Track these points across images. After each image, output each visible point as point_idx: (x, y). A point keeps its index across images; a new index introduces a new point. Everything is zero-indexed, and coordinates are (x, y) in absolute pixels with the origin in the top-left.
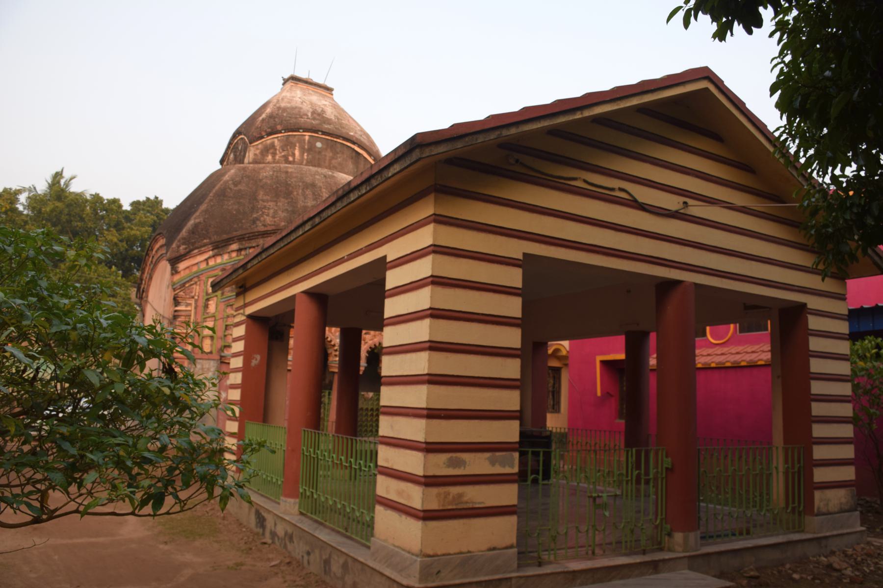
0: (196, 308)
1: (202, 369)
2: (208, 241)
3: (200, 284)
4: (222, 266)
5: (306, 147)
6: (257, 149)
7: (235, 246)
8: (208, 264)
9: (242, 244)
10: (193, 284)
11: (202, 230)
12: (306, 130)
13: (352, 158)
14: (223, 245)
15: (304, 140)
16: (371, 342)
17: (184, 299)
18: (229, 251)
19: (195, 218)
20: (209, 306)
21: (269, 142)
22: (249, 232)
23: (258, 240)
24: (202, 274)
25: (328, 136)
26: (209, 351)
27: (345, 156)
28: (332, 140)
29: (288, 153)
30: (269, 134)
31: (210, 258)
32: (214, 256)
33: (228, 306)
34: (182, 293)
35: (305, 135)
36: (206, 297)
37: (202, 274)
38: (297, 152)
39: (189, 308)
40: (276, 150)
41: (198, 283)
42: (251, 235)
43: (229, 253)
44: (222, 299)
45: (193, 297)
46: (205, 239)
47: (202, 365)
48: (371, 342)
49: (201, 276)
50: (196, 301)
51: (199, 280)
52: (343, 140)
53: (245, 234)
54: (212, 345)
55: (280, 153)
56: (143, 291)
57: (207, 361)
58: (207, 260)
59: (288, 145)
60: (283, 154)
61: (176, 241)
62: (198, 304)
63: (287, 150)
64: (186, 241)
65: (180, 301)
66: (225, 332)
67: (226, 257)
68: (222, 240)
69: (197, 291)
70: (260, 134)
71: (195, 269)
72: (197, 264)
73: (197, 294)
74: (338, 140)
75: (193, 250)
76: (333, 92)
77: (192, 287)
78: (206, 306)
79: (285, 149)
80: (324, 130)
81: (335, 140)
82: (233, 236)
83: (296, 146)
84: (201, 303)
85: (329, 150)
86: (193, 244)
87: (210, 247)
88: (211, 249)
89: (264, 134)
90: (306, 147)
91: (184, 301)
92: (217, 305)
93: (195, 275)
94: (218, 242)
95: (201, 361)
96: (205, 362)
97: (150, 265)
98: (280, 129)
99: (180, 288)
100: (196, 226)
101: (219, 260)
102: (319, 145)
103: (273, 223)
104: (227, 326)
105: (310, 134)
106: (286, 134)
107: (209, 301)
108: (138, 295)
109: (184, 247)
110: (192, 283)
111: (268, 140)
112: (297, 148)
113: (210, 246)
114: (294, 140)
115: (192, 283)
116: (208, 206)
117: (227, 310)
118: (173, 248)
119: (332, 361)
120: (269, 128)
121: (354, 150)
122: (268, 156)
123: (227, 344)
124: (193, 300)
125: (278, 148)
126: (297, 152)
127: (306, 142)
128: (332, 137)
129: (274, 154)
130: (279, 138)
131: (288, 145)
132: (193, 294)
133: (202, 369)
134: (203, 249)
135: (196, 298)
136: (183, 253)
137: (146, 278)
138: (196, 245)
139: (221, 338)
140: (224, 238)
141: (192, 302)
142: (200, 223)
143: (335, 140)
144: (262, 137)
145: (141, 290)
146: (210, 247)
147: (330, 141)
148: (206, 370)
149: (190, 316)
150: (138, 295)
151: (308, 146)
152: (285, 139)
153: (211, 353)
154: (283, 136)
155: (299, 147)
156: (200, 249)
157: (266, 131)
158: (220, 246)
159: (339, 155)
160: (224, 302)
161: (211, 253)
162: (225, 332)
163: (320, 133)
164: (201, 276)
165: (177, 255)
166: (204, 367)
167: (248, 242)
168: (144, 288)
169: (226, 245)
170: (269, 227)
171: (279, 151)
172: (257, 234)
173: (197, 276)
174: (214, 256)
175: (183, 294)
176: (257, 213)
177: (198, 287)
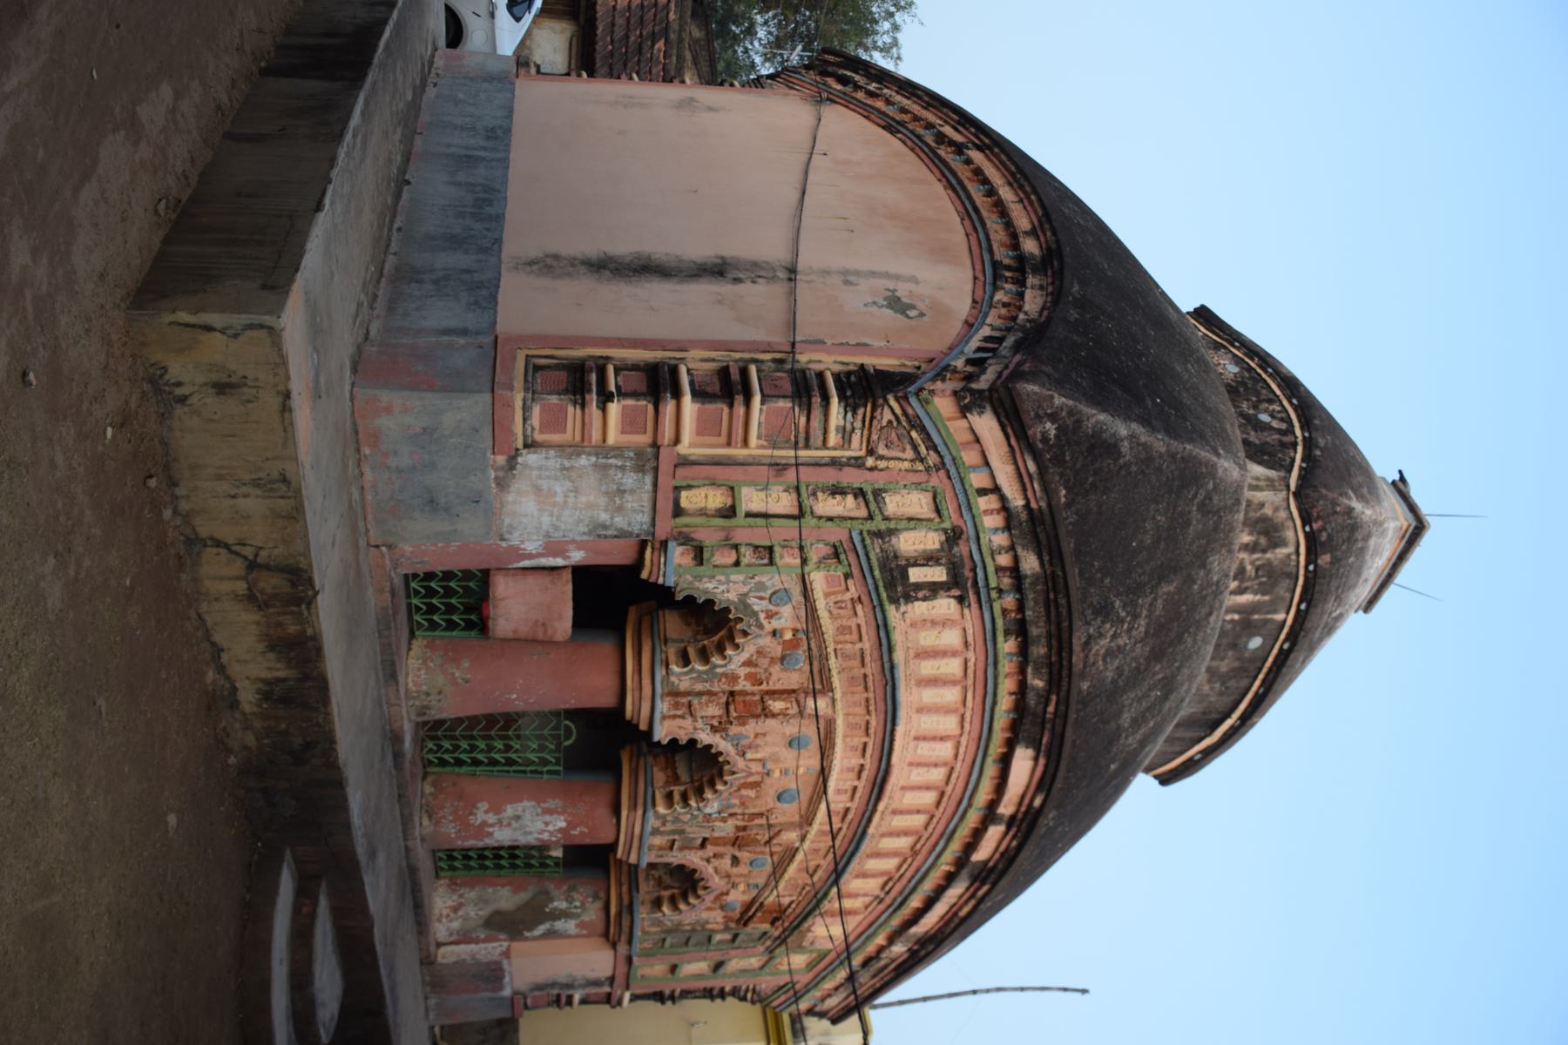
0: (834, 463)
1: (621, 492)
2: (1063, 500)
3: (917, 471)
4: (971, 532)
5: (1256, 617)
6: (1276, 509)
7: (1030, 563)
8: (982, 492)
11: (1096, 473)
12: (1301, 618)
13: (1204, 713)
14: (1042, 537)
15: (1275, 611)
16: (710, 870)
17: (868, 424)
18: (1019, 550)
19: (1132, 436)
20: (838, 497)
21: (1290, 534)
22: (1075, 606)
23: (1042, 624)
24: (949, 478)
26: (684, 503)
27: (1213, 699)
28: (1260, 669)
29: (1250, 579)
30: (1311, 538)
31: (1003, 498)
32: (1005, 508)
33: (834, 546)
34: (888, 415)
35: (1288, 612)
36: (868, 489)
37: (949, 478)
39: (833, 438)
40: (1264, 551)
41: (920, 467)
42: (1064, 611)
43: (1012, 548)
44: (861, 533)
45: (871, 452)
47: (632, 491)
48: (710, 870)
49: (942, 473)
50: (857, 463)
51: (928, 469)
52: (1257, 693)
53: (1068, 596)
54: (703, 512)
55: (1252, 563)
56: (844, 81)
57: (647, 504)
58: (996, 489)
59: (1270, 577)
60: (1249, 567)
61: (1071, 403)
62: (846, 469)
63: (1257, 577)
64: (1071, 430)
65: (861, 411)
66: (747, 545)
67: (1001, 539)
68: (1057, 537)
69: (892, 464)
70: (1319, 517)
71: (970, 457)
72: (987, 464)
73: (882, 464)
74: (1257, 683)
75: (1037, 458)
76: (1361, 612)
77: (908, 447)
78: (837, 491)
79: (1260, 573)
80: (1292, 656)
81: (1261, 676)
82: (1068, 568)
84: (852, 477)
85: (1236, 664)
86: (1058, 460)
88: (1034, 505)
89: (1315, 526)
90: (1256, 617)
91: (858, 424)
92: (844, 518)
93: (948, 460)
94: (1055, 528)
95: (649, 487)
96: (646, 498)
97: (930, 126)
98: (1320, 561)
99: (905, 413)
101: (992, 521)
102: (1256, 643)
103: (1091, 660)
104: (770, 549)
105: (1289, 622)
106: (1302, 572)
107: (856, 497)
108: (831, 58)
109: (1053, 432)
110: (923, 449)
111: (1295, 535)
112: (1258, 597)
113: (1043, 504)
114: (1282, 590)
115: (923, 449)
116: (1161, 455)
117: (821, 546)
118: (1052, 397)
119: (650, 782)
120: (1329, 535)
121: (1227, 715)
122: (1251, 534)
123: (706, 555)
124: (863, 453)
125: (1269, 555)
127: (1269, 616)
128: (1270, 669)
129: (1251, 548)
130: (1294, 557)
131: (1269, 577)
132: (882, 450)
133: (621, 492)
134: (1036, 486)
135: (870, 462)
136: (1030, 433)
137: (888, 102)
138: (1054, 472)
140: (1064, 544)
141: (856, 449)
142: (1119, 455)
143: (1261, 676)
144: (1306, 520)
145: (849, 74)
147: (1258, 665)
148: (618, 501)
149: (807, 446)
150: (831, 58)
153: (678, 511)
155: (1258, 602)
156: (1035, 476)
157: (1324, 529)
158: (1038, 530)
159: (1217, 685)
160: (851, 538)
161: (1017, 502)
162: (747, 545)
163: (1286, 646)
164: (942, 473)
165: (1029, 415)
166: (628, 497)
167: (1041, 599)
168: (857, 87)
170: (1082, 655)
171: (1258, 559)
172: (1065, 624)
173: (943, 464)
174: (1005, 508)
175: (884, 423)
176: (1124, 607)
177: (906, 465)
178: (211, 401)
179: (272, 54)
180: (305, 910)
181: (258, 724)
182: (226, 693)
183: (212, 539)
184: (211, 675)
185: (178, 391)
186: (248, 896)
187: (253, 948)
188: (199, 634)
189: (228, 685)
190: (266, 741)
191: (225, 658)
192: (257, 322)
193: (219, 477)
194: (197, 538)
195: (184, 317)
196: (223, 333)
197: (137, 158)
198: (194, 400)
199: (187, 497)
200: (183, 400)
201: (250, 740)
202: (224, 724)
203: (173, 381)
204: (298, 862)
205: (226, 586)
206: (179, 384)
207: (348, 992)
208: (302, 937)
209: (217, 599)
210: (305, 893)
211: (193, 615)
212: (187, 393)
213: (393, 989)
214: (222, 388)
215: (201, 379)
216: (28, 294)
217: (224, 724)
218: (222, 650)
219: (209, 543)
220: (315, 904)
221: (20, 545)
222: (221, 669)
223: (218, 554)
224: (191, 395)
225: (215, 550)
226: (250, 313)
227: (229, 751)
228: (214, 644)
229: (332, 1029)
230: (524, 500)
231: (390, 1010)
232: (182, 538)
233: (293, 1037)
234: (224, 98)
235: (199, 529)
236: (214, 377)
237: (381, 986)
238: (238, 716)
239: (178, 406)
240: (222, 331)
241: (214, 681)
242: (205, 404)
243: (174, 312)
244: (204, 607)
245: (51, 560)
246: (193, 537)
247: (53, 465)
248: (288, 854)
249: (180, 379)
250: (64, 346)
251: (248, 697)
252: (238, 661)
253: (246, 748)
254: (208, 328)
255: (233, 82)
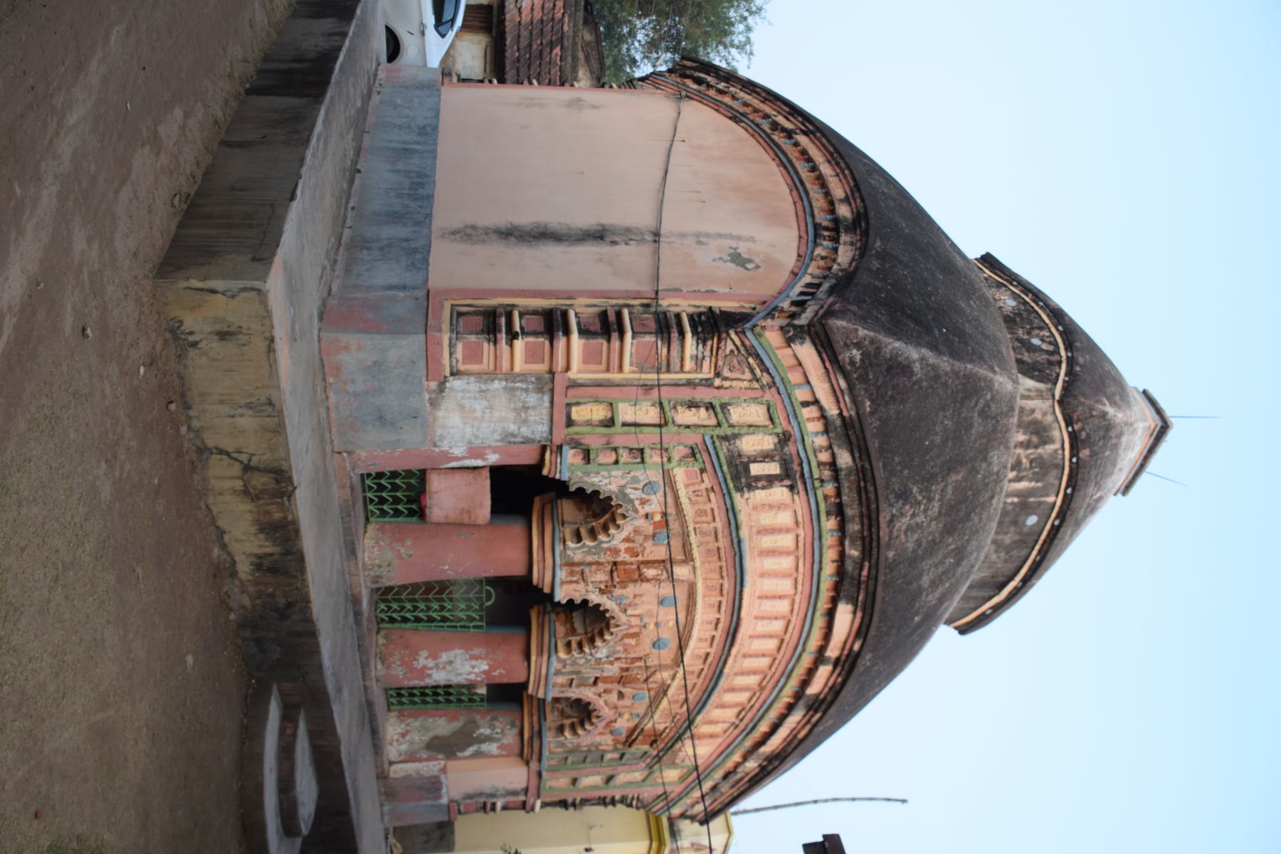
0: (689, 383)
1: (526, 408)
2: (868, 409)
4: (798, 435)
5: (1032, 500)
6: (1045, 414)
7: (844, 459)
8: (805, 404)
9: (848, 475)
10: (752, 371)
11: (894, 388)
12: (1068, 500)
13: (993, 577)
14: (853, 438)
15: (1047, 495)
16: (601, 702)
18: (836, 449)
21: (1056, 434)
22: (880, 492)
23: (855, 506)
24: (779, 393)
25: (1048, 536)
26: (574, 416)
27: (999, 565)
28: (1036, 542)
30: (1074, 437)
31: (821, 409)
32: (823, 417)
33: (692, 448)
34: (730, 346)
35: (1057, 496)
36: (716, 403)
37: (779, 393)
38: (1023, 485)
39: (688, 364)
40: (1036, 447)
41: (756, 385)
42: (872, 496)
43: (830, 447)
44: (712, 437)
45: (718, 375)
46: (872, 401)
47: (534, 408)
48: (601, 702)
49: (773, 390)
50: (707, 383)
51: (762, 387)
52: (1034, 561)
53: (874, 484)
54: (589, 423)
55: (1027, 457)
56: (699, 81)
57: (546, 418)
58: (816, 402)
59: (1042, 468)
60: (1024, 461)
61: (872, 334)
62: (699, 388)
63: (1031, 468)
64: (872, 356)
65: (709, 343)
66: (624, 447)
67: (821, 441)
68: (864, 438)
69: (734, 383)
70: (1079, 420)
71: (795, 377)
72: (808, 382)
73: (727, 384)
74: (1035, 553)
75: (846, 376)
76: (1119, 495)
77: (747, 370)
78: (692, 405)
79: (1034, 465)
80: (1062, 530)
81: (1037, 547)
83: (1037, 481)
84: (703, 394)
85: (1017, 538)
86: (863, 379)
87: (849, 412)
88: (845, 414)
89: (1077, 427)
90: (1032, 500)
91: (707, 353)
92: (699, 426)
93: (777, 380)
94: (862, 431)
95: (547, 404)
96: (545, 413)
97: (766, 116)
98: (1081, 455)
100: (906, 369)
101: (814, 427)
102: (1032, 520)
103: (895, 534)
104: (642, 451)
106: (1067, 463)
107: (707, 409)
108: (689, 63)
109: (858, 358)
110: (758, 372)
111: (1060, 435)
112: (1033, 484)
113: (853, 413)
114: (1051, 478)
115: (758, 372)
116: (946, 374)
118: (857, 330)
119: (553, 634)
120: (1087, 434)
121: (1011, 578)
122: (1025, 433)
123: (592, 456)
124: (712, 375)
125: (1040, 451)
126: (1023, 485)
127: (1042, 499)
129: (1026, 445)
130: (1060, 452)
131: (1041, 468)
132: (726, 373)
133: (526, 408)
134: (847, 398)
135: (717, 382)
136: (840, 358)
137: (734, 98)
139: (608, 443)
140: (870, 444)
141: (707, 372)
143: (1037, 547)
144: (1069, 422)
145: (702, 75)
146: (849, 412)
147: (1035, 537)
148: (523, 415)
149: (668, 371)
150: (689, 63)
151: (1033, 503)
152: (1059, 461)
153: (570, 423)
154: (1063, 459)
155: (1033, 488)
156: (846, 391)
157: (1083, 429)
158: (850, 433)
159: (1003, 555)
160: (704, 441)
161: (833, 411)
162: (624, 447)
163: (1057, 523)
164: (773, 390)
165: (839, 346)
166: (531, 412)
167: (854, 487)
168: (709, 86)
169: (851, 444)
170: (887, 530)
171: (1031, 454)
172: (874, 506)
173: (774, 383)
174: (823, 417)
175: (728, 352)
176: (920, 493)
177: (746, 384)
178: (216, 346)
179: (255, 78)
180: (289, 732)
181: (251, 589)
182: (227, 565)
183: (217, 448)
184: (216, 551)
185: (191, 338)
186: (245, 721)
187: (249, 762)
188: (208, 520)
189: (229, 559)
190: (258, 602)
191: (226, 538)
192: (248, 286)
193: (222, 402)
194: (205, 448)
195: (195, 283)
196: (224, 295)
197: (159, 166)
198: (202, 345)
199: (198, 417)
200: (194, 345)
201: (246, 601)
202: (226, 588)
203: (187, 331)
204: (283, 696)
205: (227, 484)
206: (191, 333)
207: (321, 796)
208: (286, 752)
209: (220, 494)
210: (288, 718)
211: (203, 506)
212: (198, 339)
213: (356, 795)
214: (223, 336)
215: (208, 329)
216: (86, 271)
217: (226, 588)
218: (224, 532)
219: (215, 451)
220: (296, 727)
221: (82, 454)
222: (224, 547)
223: (221, 460)
224: (201, 341)
225: (218, 457)
226: (244, 279)
227: (230, 609)
228: (218, 528)
229: (310, 824)
230: (390, 416)
231: (353, 812)
232: (194, 448)
233: (281, 828)
234: (220, 114)
235: (206, 441)
236: (218, 327)
237: (347, 792)
238: (237, 582)
239: (191, 349)
240: (224, 293)
241: (219, 556)
242: (211, 347)
243: (188, 279)
244: (211, 500)
245: (103, 464)
246: (202, 447)
247: (104, 396)
248: (275, 688)
249: (192, 329)
250: (110, 307)
251: (244, 568)
252: (236, 540)
253: (243, 607)
254: (213, 291)
255: (226, 101)
